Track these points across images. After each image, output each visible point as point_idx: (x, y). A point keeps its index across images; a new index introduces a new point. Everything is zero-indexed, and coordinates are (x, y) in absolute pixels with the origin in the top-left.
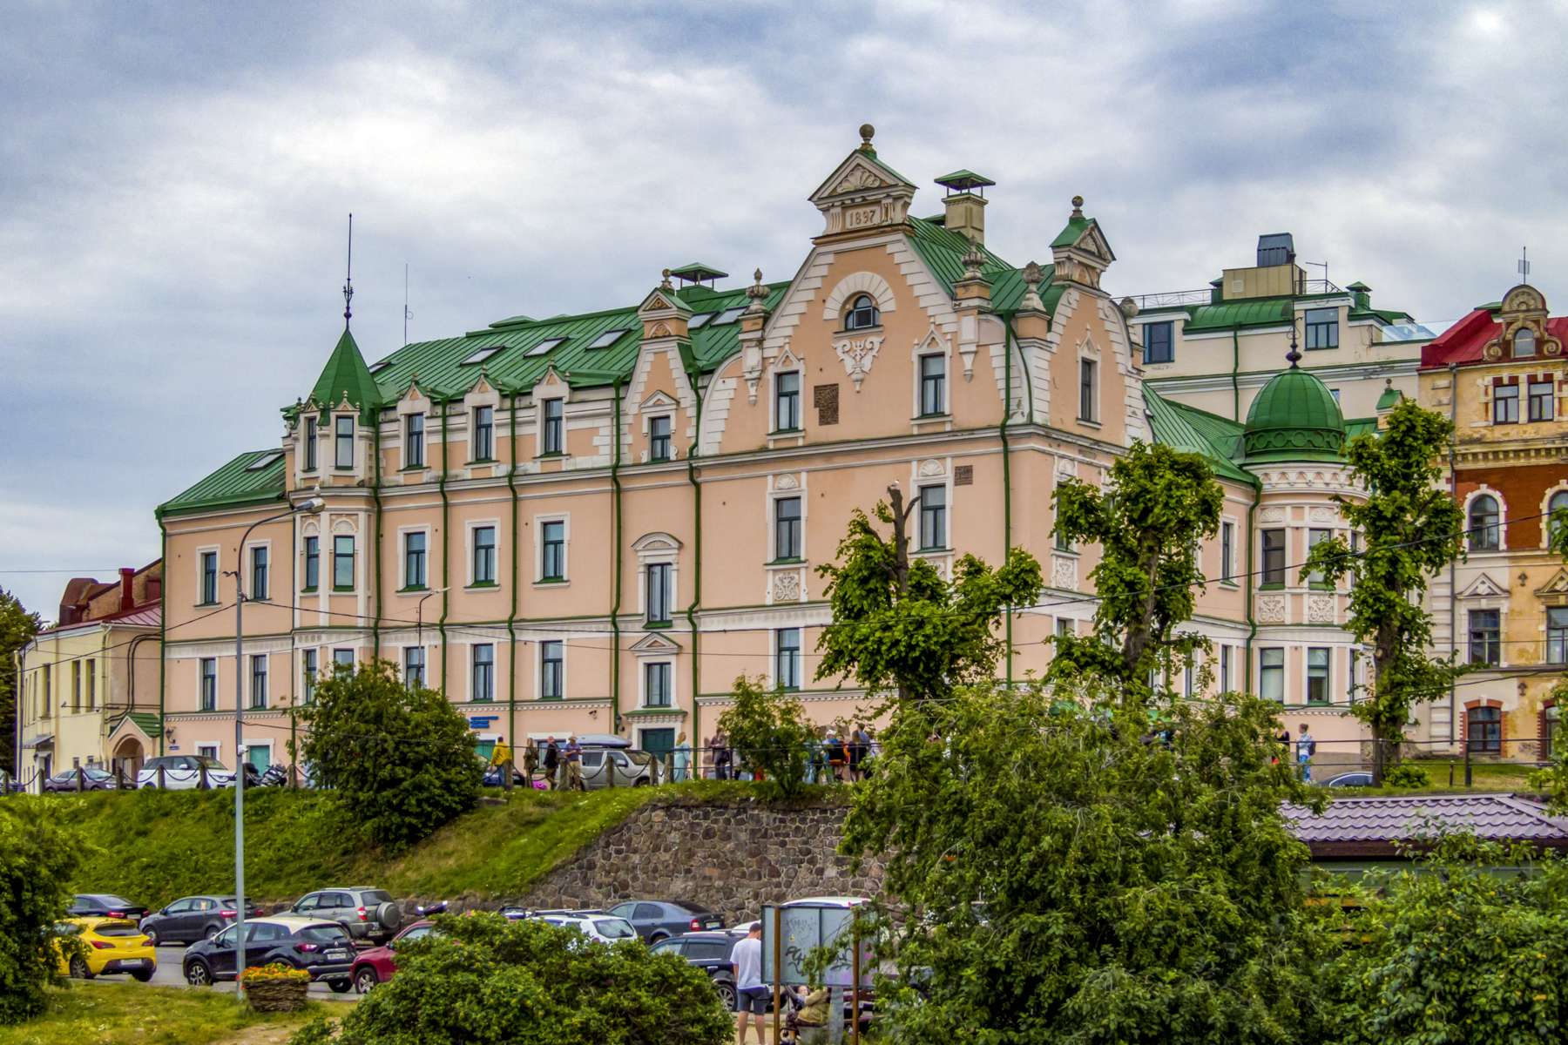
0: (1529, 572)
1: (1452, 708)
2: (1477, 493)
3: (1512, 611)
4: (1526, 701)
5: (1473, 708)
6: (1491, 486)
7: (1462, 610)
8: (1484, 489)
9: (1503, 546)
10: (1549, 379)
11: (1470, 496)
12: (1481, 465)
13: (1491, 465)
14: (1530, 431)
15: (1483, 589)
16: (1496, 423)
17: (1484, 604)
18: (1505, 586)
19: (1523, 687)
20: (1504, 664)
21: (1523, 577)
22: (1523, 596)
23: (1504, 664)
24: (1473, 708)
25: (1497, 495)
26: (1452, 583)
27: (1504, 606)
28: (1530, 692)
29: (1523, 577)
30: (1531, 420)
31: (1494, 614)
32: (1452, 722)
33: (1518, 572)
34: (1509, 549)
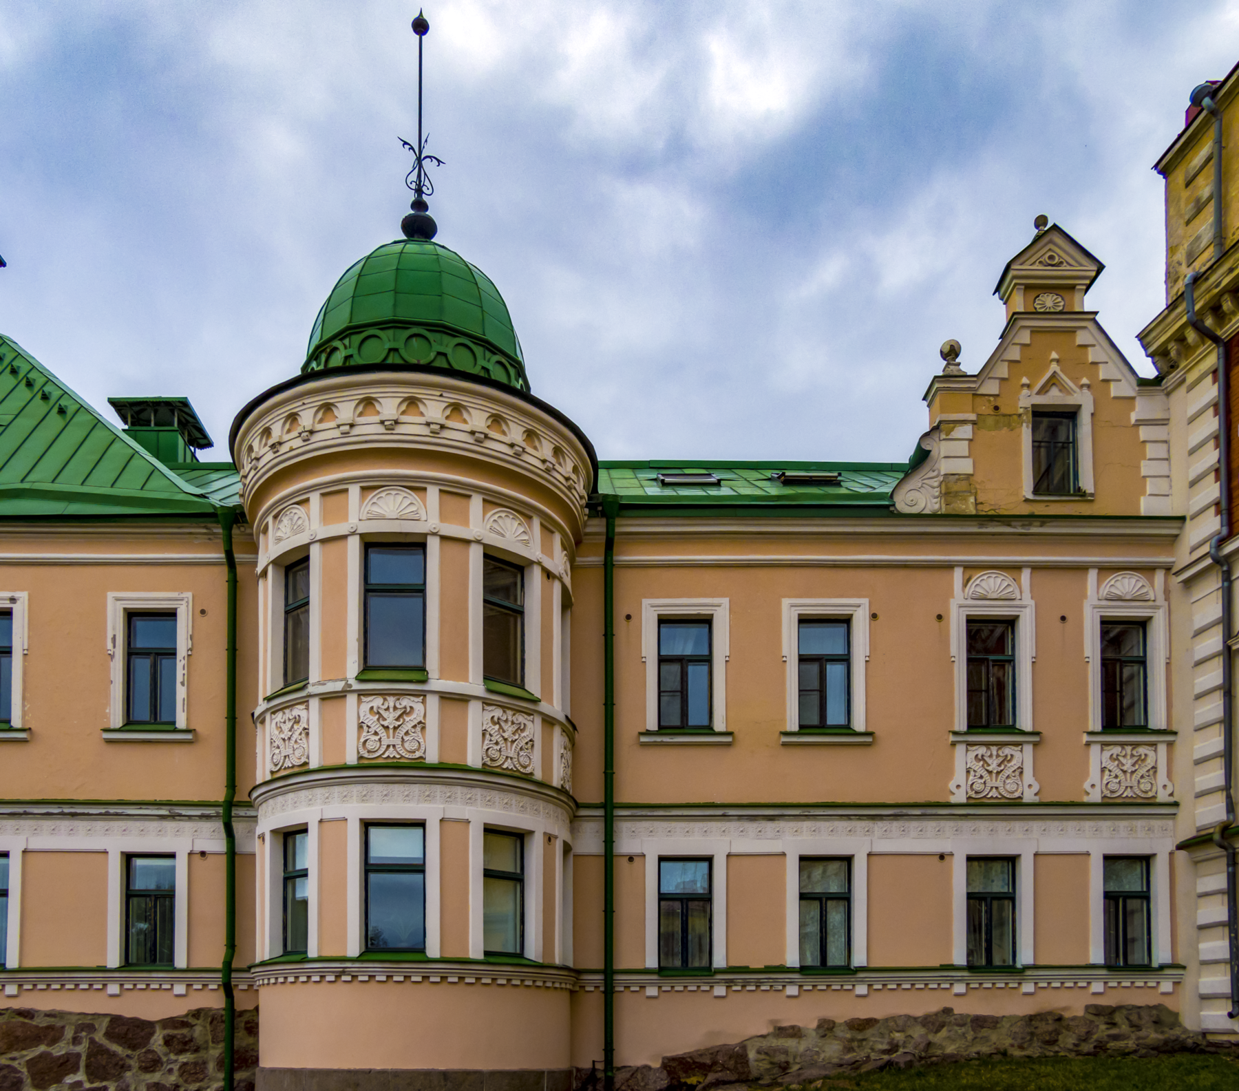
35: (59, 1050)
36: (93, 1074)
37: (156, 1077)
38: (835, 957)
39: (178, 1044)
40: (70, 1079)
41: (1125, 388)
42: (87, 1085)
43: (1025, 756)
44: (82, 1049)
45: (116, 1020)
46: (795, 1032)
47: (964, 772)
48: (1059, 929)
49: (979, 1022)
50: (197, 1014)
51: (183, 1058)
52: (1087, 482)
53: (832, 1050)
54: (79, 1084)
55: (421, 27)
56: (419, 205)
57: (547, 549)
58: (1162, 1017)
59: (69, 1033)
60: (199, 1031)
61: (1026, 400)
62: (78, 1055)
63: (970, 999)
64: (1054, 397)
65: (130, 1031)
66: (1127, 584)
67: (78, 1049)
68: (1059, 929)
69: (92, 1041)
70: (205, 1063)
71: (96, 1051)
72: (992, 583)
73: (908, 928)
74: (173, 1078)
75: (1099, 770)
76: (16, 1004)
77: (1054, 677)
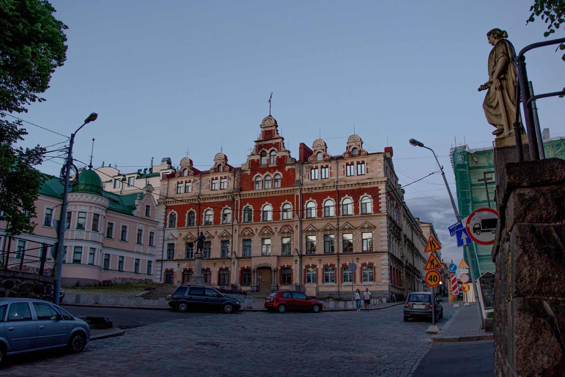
0: (182, 233)
1: (161, 270)
3: (177, 244)
4: (179, 269)
5: (167, 271)
6: (175, 210)
7: (166, 243)
8: (173, 211)
9: (176, 226)
10: (190, 181)
11: (170, 213)
12: (172, 204)
13: (175, 204)
14: (185, 195)
15: (171, 238)
16: (177, 193)
17: (171, 242)
18: (176, 237)
19: (179, 265)
20: (174, 259)
21: (181, 234)
22: (180, 239)
23: (174, 259)
24: (167, 271)
26: (164, 236)
27: (175, 242)
28: (180, 266)
29: (181, 234)
30: (185, 192)
31: (173, 244)
32: (161, 275)
33: (179, 233)
34: (178, 227)
38: (121, 269)
41: (155, 205)
43: (142, 247)
46: (116, 279)
47: (136, 248)
48: (143, 268)
49: (135, 279)
52: (150, 215)
53: (120, 282)
55: (94, 140)
56: (91, 164)
57: (102, 212)
58: (151, 281)
61: (146, 204)
63: (134, 276)
64: (148, 204)
66: (153, 228)
68: (143, 268)
72: (141, 225)
73: (129, 267)
75: (149, 250)
77: (145, 239)
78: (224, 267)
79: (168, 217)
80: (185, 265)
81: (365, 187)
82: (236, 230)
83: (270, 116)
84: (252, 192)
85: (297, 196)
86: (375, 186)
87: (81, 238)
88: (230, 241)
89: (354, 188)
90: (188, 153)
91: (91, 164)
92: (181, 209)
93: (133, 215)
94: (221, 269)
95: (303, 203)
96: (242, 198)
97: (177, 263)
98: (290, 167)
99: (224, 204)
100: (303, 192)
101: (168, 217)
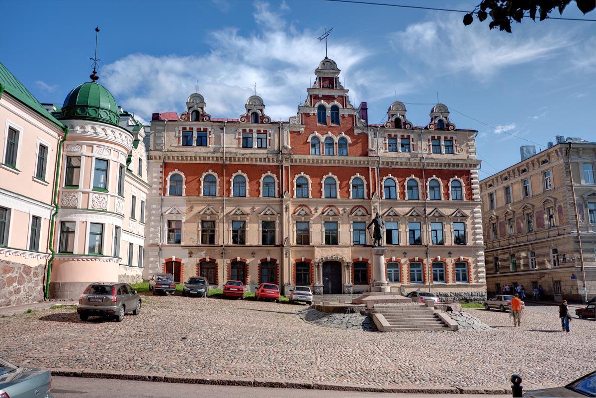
2: (173, 172)
8: (176, 171)
9: (184, 194)
11: (171, 174)
23: (183, 243)
25: (182, 174)
35: (14, 275)
36: (20, 283)
37: (29, 285)
39: (36, 275)
40: (14, 284)
42: (18, 287)
44: (17, 275)
45: (25, 266)
50: (39, 266)
51: (36, 279)
54: (16, 286)
55: (97, 30)
56: (94, 72)
59: (16, 270)
60: (39, 271)
62: (16, 277)
65: (27, 269)
67: (17, 275)
69: (20, 273)
70: (39, 280)
71: (21, 276)
74: (33, 285)
76: (7, 259)
78: (269, 259)
79: (168, 179)
80: (202, 253)
81: (456, 168)
82: (287, 208)
83: (326, 58)
84: (310, 157)
85: (373, 170)
86: (468, 168)
87: (103, 207)
88: (277, 222)
89: (443, 168)
90: (197, 88)
91: (94, 72)
92: (193, 169)
93: (131, 171)
94: (264, 262)
95: (381, 180)
96: (293, 164)
97: (187, 251)
98: (360, 131)
99: (264, 169)
100: (381, 166)
101: (168, 179)
